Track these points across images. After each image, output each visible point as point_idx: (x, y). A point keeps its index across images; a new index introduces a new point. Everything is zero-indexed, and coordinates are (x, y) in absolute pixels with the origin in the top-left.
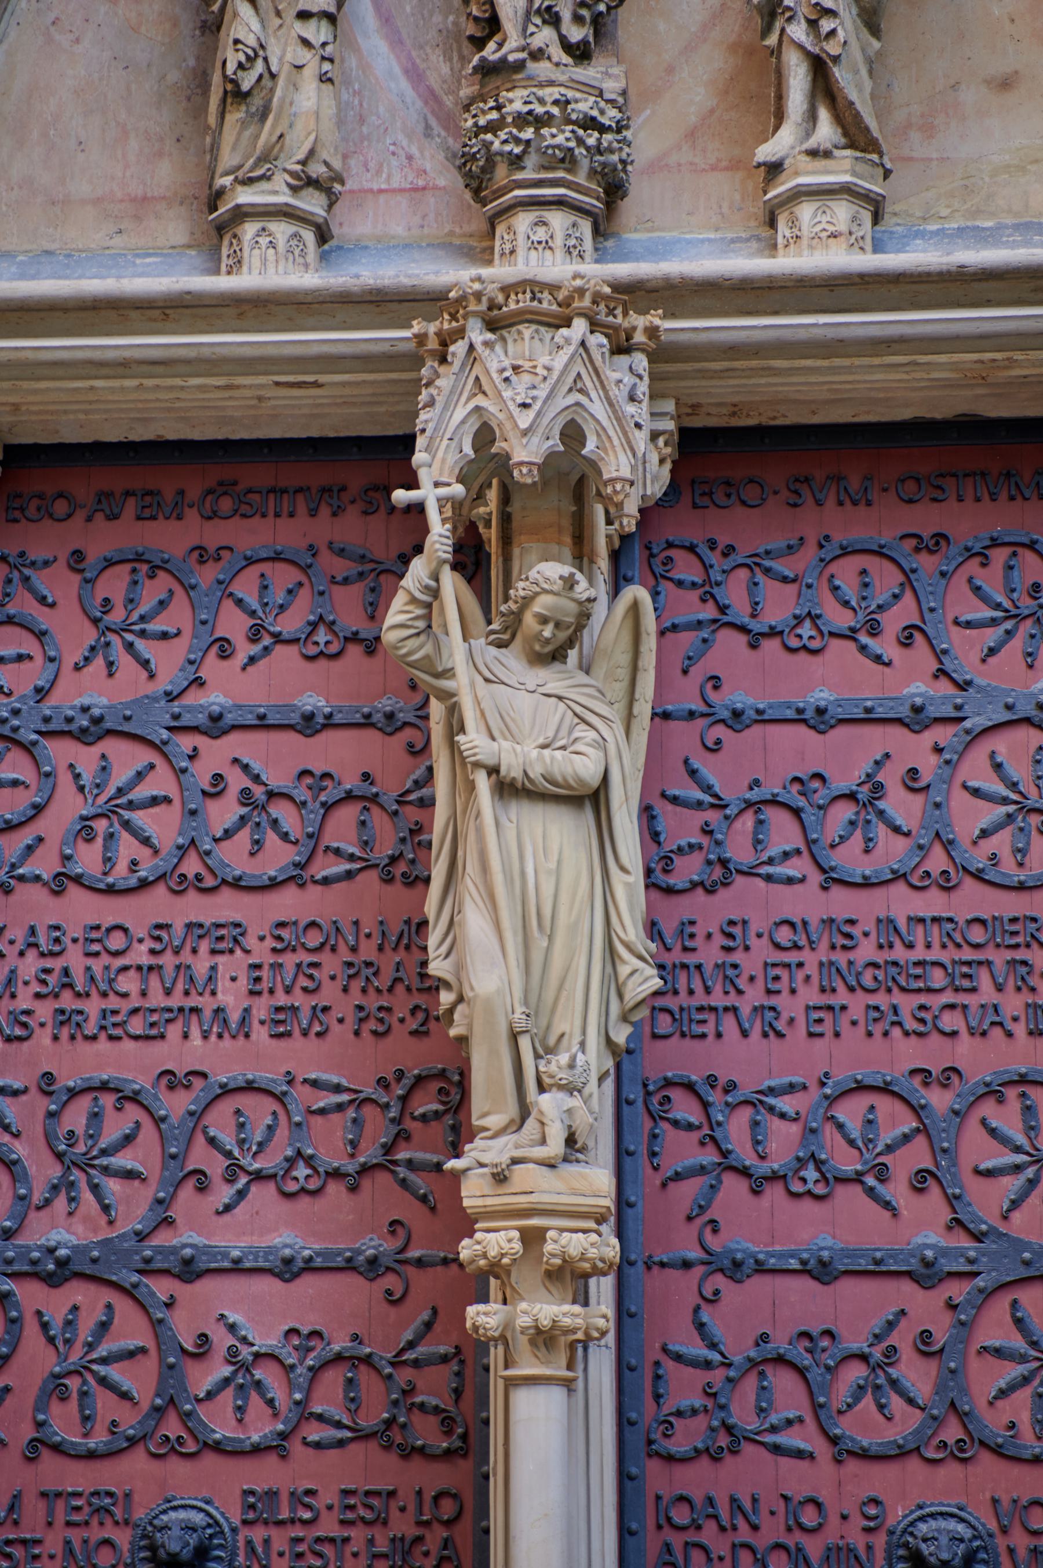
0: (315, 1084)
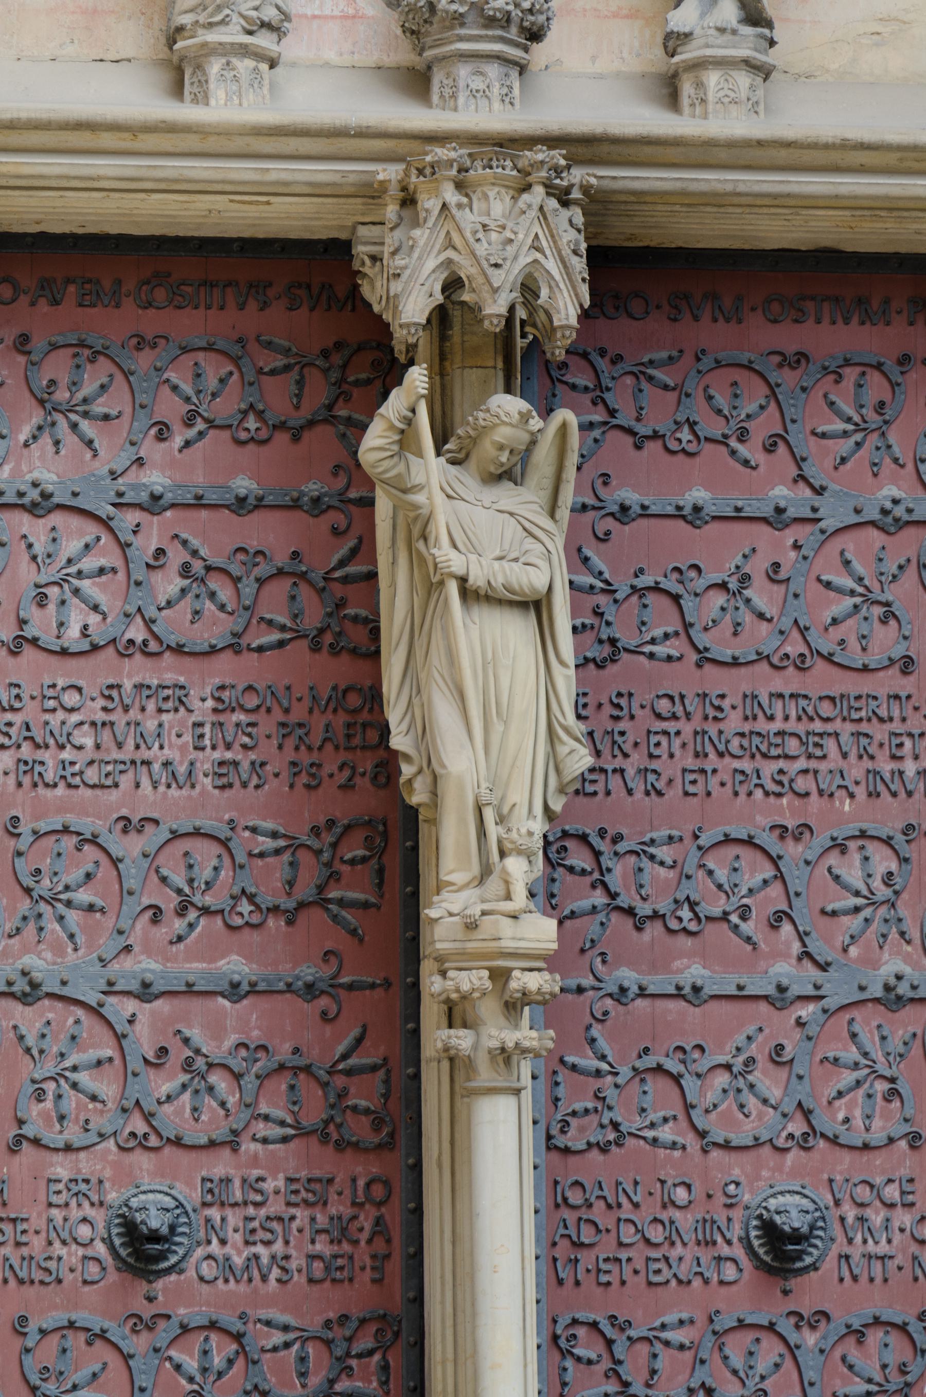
0: (254, 830)
